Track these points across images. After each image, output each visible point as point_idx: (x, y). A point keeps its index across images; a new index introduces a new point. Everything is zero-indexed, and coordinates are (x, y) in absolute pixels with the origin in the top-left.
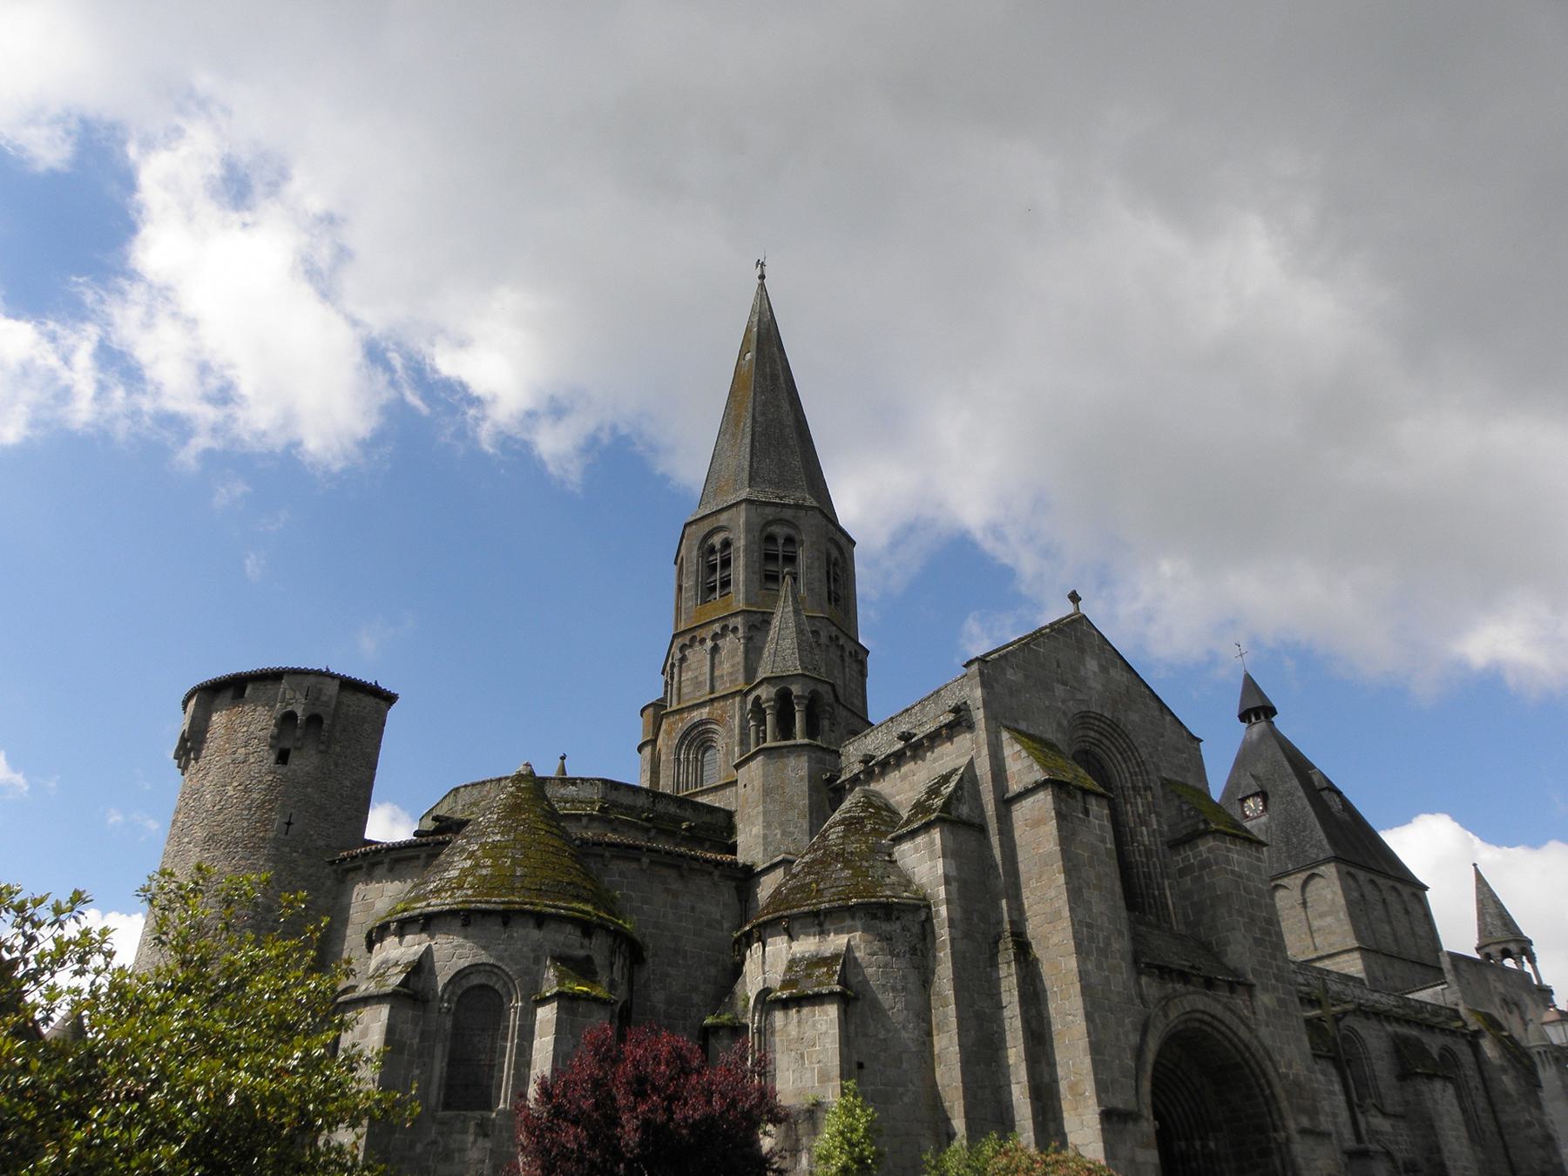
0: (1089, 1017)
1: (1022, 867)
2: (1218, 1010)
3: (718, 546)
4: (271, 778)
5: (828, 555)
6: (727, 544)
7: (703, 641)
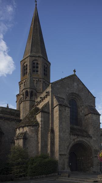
0: (59, 141)
1: (54, 119)
2: (85, 141)
3: (25, 66)
5: (44, 67)
6: (27, 65)
7: (23, 83)
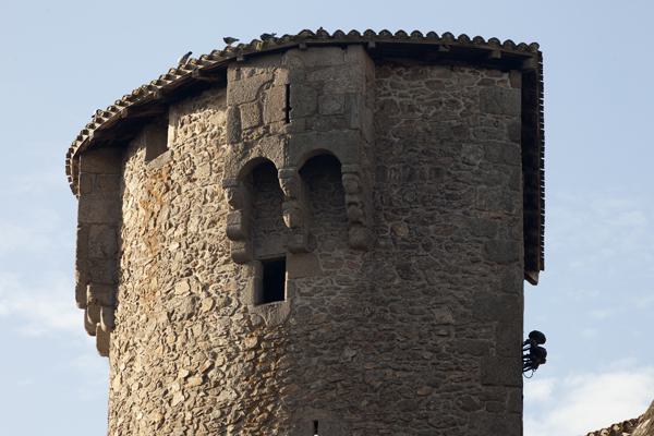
4: (252, 342)
